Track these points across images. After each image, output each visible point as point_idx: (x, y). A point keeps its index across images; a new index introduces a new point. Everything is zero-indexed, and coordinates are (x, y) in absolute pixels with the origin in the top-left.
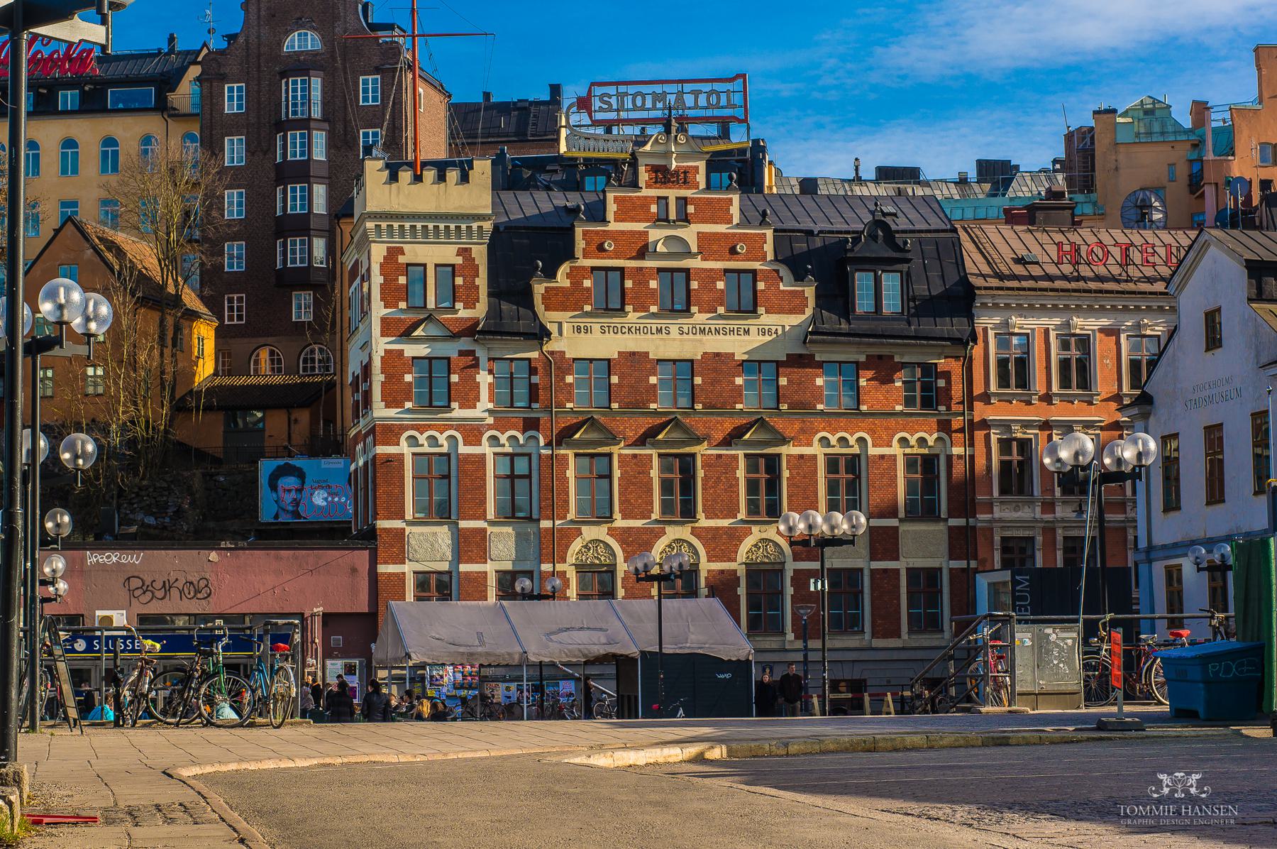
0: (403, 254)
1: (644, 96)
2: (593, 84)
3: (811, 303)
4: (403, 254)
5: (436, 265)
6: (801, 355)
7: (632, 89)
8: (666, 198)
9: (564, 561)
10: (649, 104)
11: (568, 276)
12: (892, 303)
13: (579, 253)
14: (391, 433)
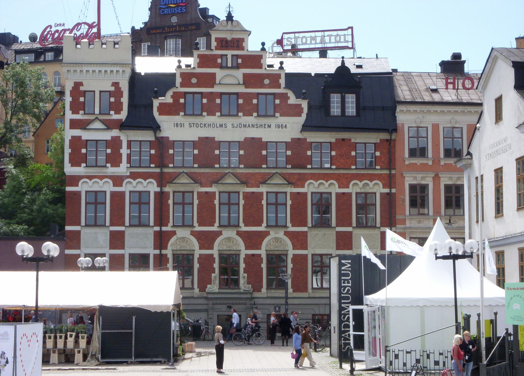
0: (82, 85)
1: (306, 38)
2: (284, 33)
3: (305, 110)
4: (82, 85)
5: (101, 92)
6: (299, 139)
7: (301, 35)
8: (227, 55)
9: (166, 249)
10: (309, 42)
11: (172, 97)
12: (351, 110)
13: (178, 84)
14: (75, 180)
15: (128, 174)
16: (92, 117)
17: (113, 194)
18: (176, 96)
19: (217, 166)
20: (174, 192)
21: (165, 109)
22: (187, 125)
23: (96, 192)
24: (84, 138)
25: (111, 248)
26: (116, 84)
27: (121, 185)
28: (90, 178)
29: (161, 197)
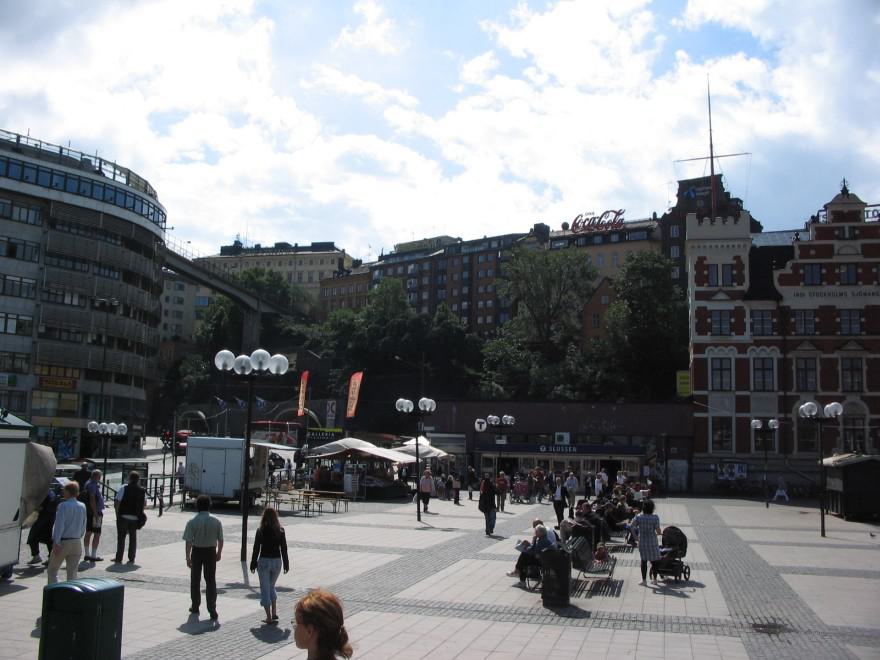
15: (752, 342)
16: (716, 289)
17: (738, 361)
18: (796, 267)
19: (793, 333)
20: (797, 358)
21: (785, 280)
22: (807, 294)
23: (721, 359)
24: (709, 309)
25: (737, 411)
26: (737, 258)
27: (746, 352)
28: (716, 345)
29: (784, 364)
